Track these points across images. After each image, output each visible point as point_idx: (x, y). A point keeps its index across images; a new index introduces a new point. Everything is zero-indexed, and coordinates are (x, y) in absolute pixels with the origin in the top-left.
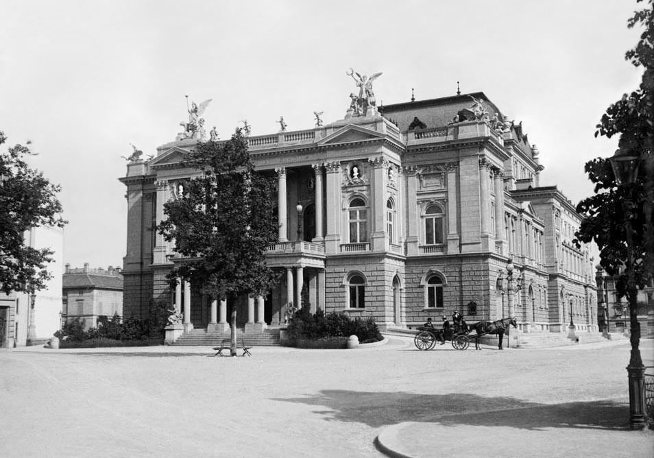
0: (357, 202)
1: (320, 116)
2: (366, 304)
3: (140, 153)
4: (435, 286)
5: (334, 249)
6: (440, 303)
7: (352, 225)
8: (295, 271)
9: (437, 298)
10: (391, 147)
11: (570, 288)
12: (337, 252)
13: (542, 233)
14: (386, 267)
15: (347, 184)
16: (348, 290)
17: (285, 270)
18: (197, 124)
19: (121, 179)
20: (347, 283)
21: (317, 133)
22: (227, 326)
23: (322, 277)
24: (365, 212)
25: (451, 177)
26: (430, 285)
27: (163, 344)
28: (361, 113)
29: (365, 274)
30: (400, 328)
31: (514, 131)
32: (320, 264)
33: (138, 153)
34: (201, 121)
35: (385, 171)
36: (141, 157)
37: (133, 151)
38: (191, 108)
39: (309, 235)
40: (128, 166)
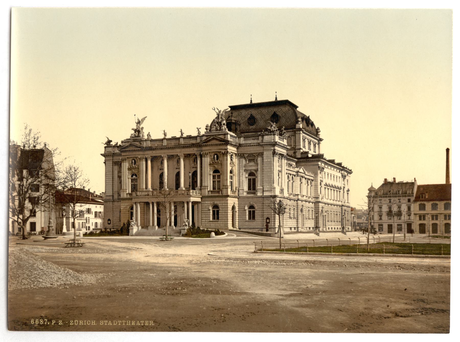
0: (216, 171)
1: (200, 130)
2: (220, 218)
3: (111, 141)
4: (252, 210)
5: (206, 193)
6: (254, 218)
7: (214, 182)
8: (188, 203)
9: (252, 216)
10: (232, 145)
11: (326, 208)
12: (207, 194)
13: (313, 180)
14: (229, 202)
15: (211, 162)
16: (211, 212)
17: (183, 203)
18: (140, 130)
19: (101, 155)
20: (211, 208)
21: (198, 138)
22: (157, 227)
23: (200, 205)
24: (220, 176)
25: (259, 159)
26: (250, 210)
27: (128, 235)
28: (219, 129)
29: (219, 205)
30: (235, 229)
31: (304, 122)
32: (199, 200)
33: (109, 142)
34: (142, 128)
35: (229, 158)
36: (111, 143)
37: (106, 140)
38: (137, 121)
39: (193, 185)
40: (105, 147)
